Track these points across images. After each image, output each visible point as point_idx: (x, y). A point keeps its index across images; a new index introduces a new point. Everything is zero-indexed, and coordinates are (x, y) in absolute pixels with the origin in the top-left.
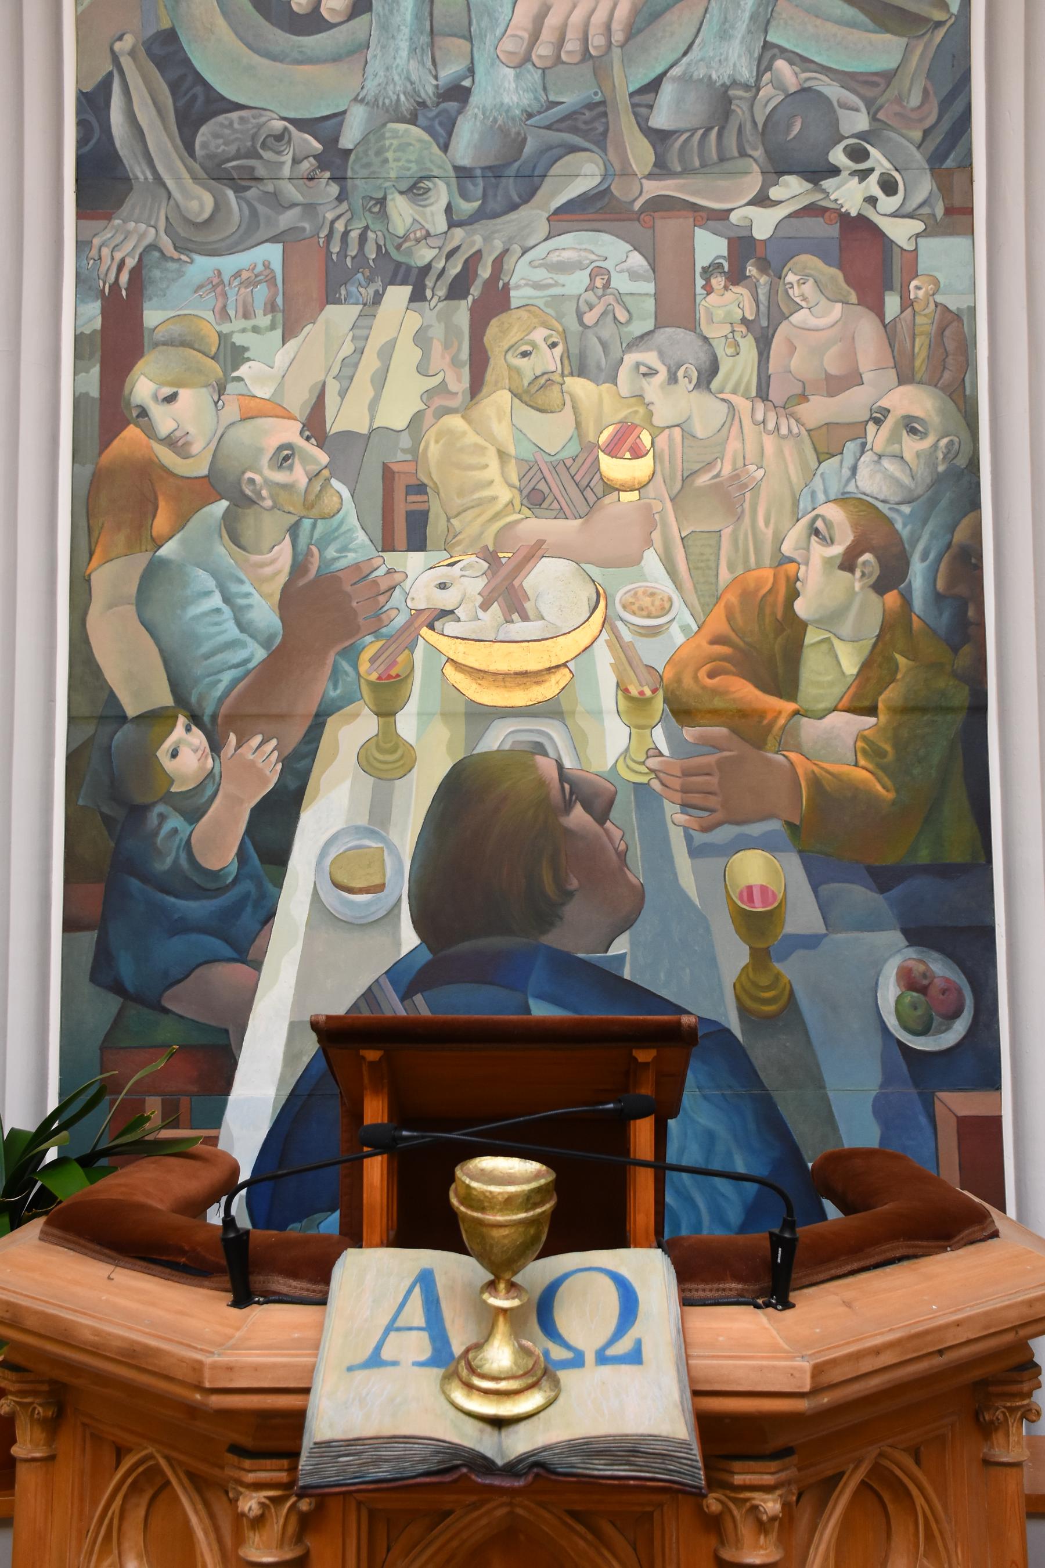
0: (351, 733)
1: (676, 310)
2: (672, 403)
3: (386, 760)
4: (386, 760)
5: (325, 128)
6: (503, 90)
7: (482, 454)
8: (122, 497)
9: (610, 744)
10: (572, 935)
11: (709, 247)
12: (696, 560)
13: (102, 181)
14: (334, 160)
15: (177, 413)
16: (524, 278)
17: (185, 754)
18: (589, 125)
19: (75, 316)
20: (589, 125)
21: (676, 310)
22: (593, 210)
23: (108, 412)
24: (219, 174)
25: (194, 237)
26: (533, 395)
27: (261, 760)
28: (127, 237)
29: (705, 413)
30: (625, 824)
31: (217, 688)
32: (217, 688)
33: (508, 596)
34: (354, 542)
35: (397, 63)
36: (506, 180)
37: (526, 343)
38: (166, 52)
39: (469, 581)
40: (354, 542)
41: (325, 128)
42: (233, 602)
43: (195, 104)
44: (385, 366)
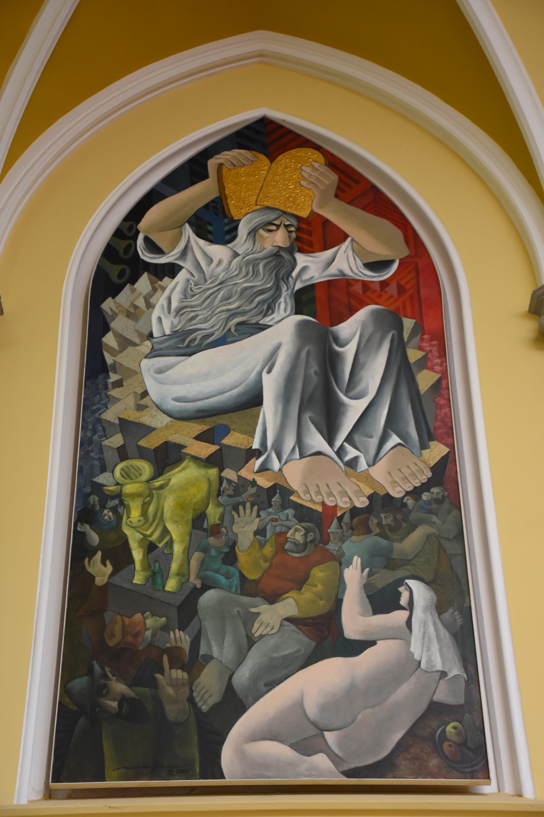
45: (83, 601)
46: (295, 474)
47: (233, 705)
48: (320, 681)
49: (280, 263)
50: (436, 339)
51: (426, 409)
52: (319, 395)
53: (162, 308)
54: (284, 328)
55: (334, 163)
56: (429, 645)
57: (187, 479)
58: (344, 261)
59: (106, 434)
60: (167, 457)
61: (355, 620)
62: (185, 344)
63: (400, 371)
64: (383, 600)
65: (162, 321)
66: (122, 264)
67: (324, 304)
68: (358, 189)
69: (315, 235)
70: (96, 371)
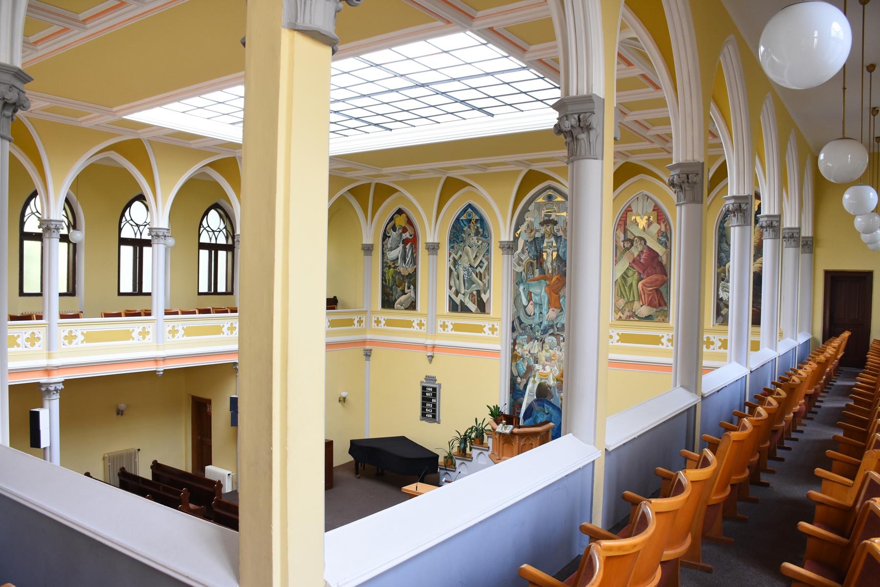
0: (532, 379)
1: (558, 344)
2: (558, 353)
3: (534, 382)
4: (534, 382)
5: (531, 325)
6: (545, 323)
7: (542, 356)
8: (515, 357)
9: (551, 382)
10: (548, 398)
11: (561, 338)
12: (560, 366)
13: (513, 329)
14: (531, 328)
15: (519, 350)
16: (546, 341)
17: (519, 380)
18: (552, 327)
19: (512, 341)
20: (552, 327)
21: (558, 344)
22: (552, 334)
23: (514, 350)
24: (522, 329)
25: (521, 335)
26: (547, 351)
27: (525, 381)
28: (515, 334)
29: (560, 354)
30: (552, 390)
31: (521, 374)
32: (521, 374)
33: (544, 369)
34: (532, 363)
35: (537, 320)
36: (545, 331)
37: (547, 346)
38: (519, 318)
39: (541, 367)
40: (532, 363)
41: (531, 325)
42: (523, 368)
43: (521, 323)
44: (535, 347)
45: (383, 287)
46: (401, 269)
47: (396, 300)
48: (403, 298)
49: (401, 235)
50: (415, 247)
51: (414, 261)
52: (404, 260)
53: (389, 243)
54: (401, 245)
55: (407, 217)
56: (413, 295)
57: (391, 270)
58: (406, 235)
59: (385, 265)
60: (390, 267)
61: (406, 291)
62: (391, 249)
63: (412, 254)
64: (409, 288)
65: (389, 246)
66: (385, 237)
67: (405, 242)
68: (410, 222)
69: (405, 230)
70: (383, 253)
